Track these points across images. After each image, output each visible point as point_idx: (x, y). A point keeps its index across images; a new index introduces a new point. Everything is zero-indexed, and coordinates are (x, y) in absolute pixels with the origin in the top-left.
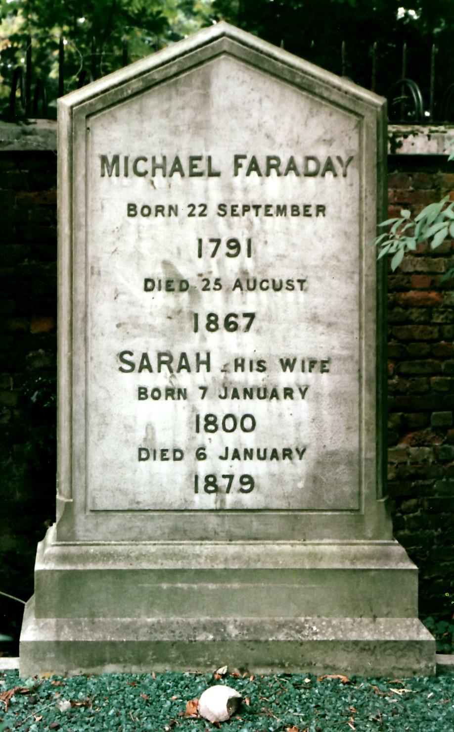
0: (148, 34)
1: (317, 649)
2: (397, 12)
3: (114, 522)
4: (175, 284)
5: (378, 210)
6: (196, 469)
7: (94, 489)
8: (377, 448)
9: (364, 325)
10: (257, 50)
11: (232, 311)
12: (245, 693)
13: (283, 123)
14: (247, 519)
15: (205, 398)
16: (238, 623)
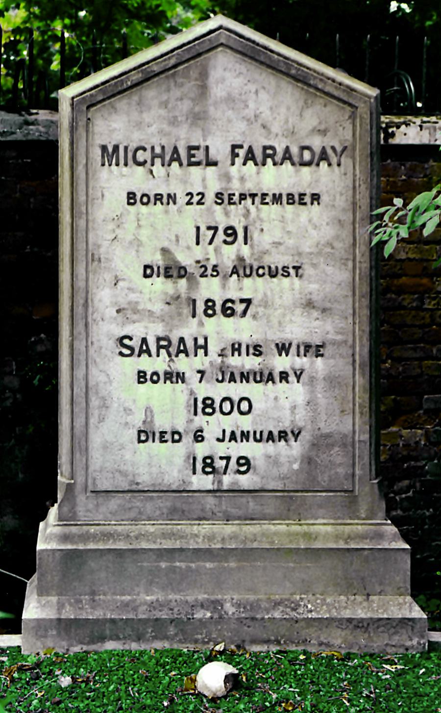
0: (147, 28)
1: (312, 626)
2: (390, 5)
3: (114, 503)
4: (173, 271)
5: (371, 198)
6: (194, 451)
7: (95, 471)
8: (370, 430)
9: (357, 310)
10: (254, 42)
11: (229, 296)
12: (241, 669)
13: (279, 114)
14: (244, 500)
15: (203, 382)
16: (234, 601)
